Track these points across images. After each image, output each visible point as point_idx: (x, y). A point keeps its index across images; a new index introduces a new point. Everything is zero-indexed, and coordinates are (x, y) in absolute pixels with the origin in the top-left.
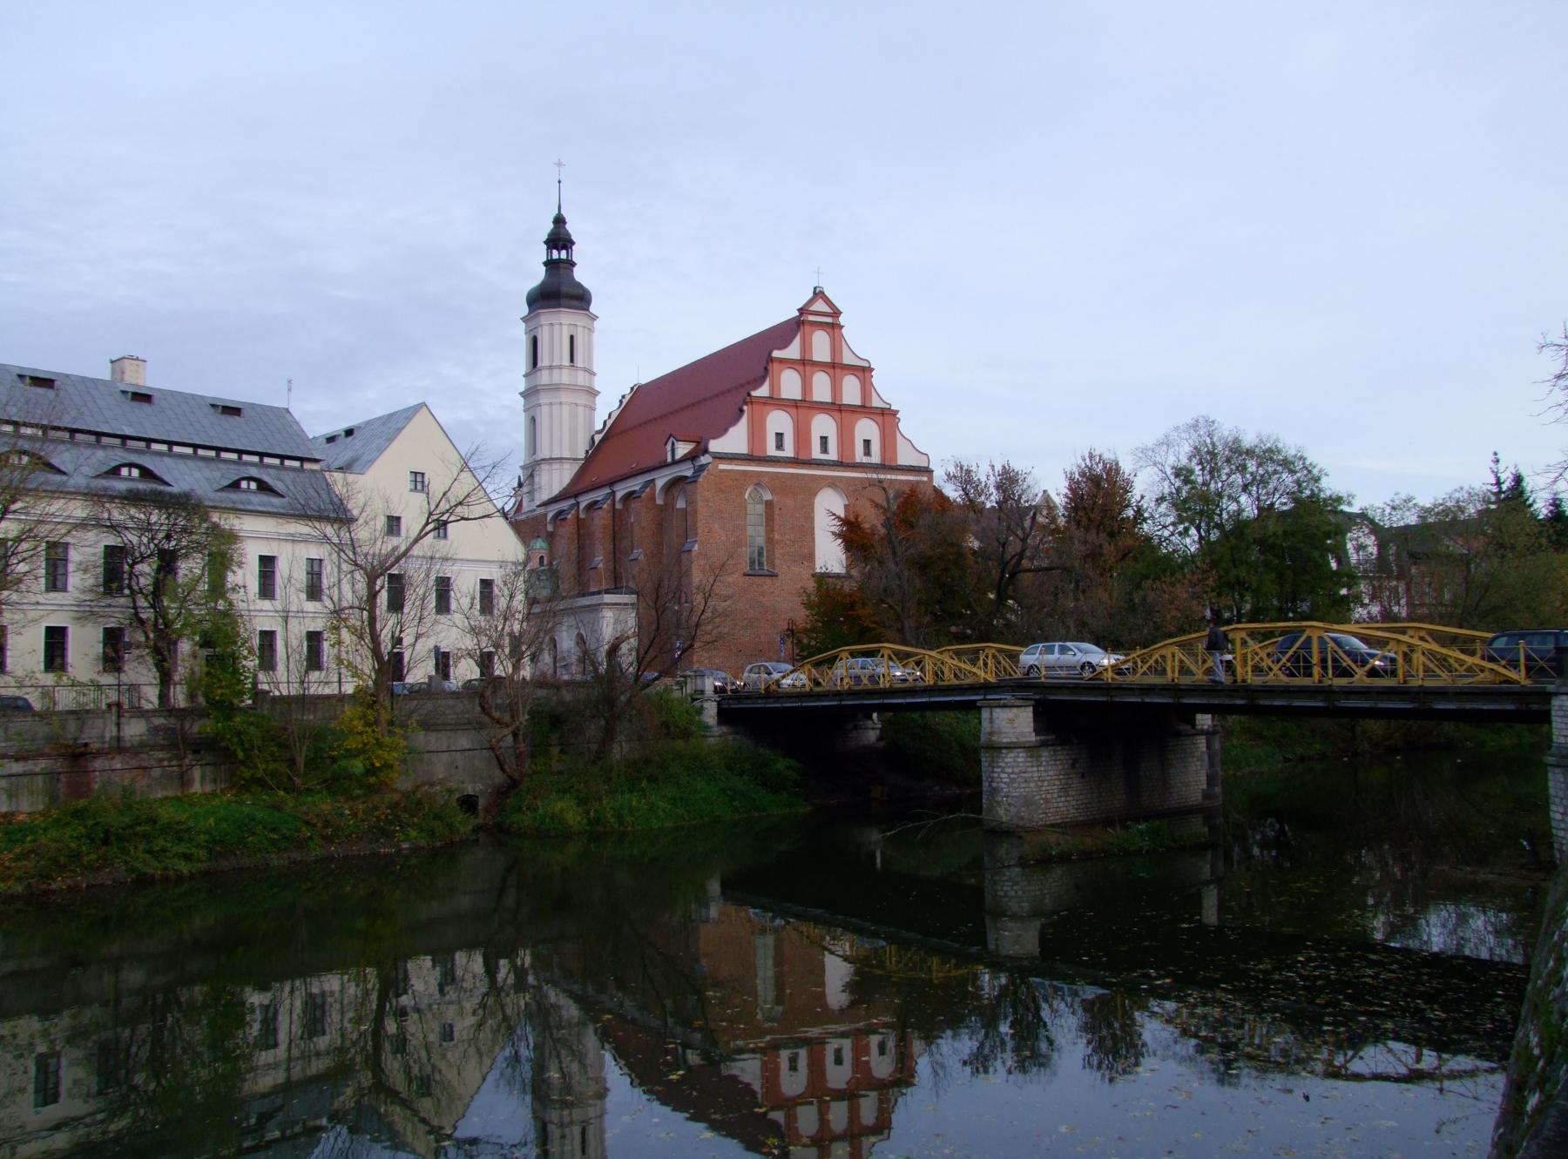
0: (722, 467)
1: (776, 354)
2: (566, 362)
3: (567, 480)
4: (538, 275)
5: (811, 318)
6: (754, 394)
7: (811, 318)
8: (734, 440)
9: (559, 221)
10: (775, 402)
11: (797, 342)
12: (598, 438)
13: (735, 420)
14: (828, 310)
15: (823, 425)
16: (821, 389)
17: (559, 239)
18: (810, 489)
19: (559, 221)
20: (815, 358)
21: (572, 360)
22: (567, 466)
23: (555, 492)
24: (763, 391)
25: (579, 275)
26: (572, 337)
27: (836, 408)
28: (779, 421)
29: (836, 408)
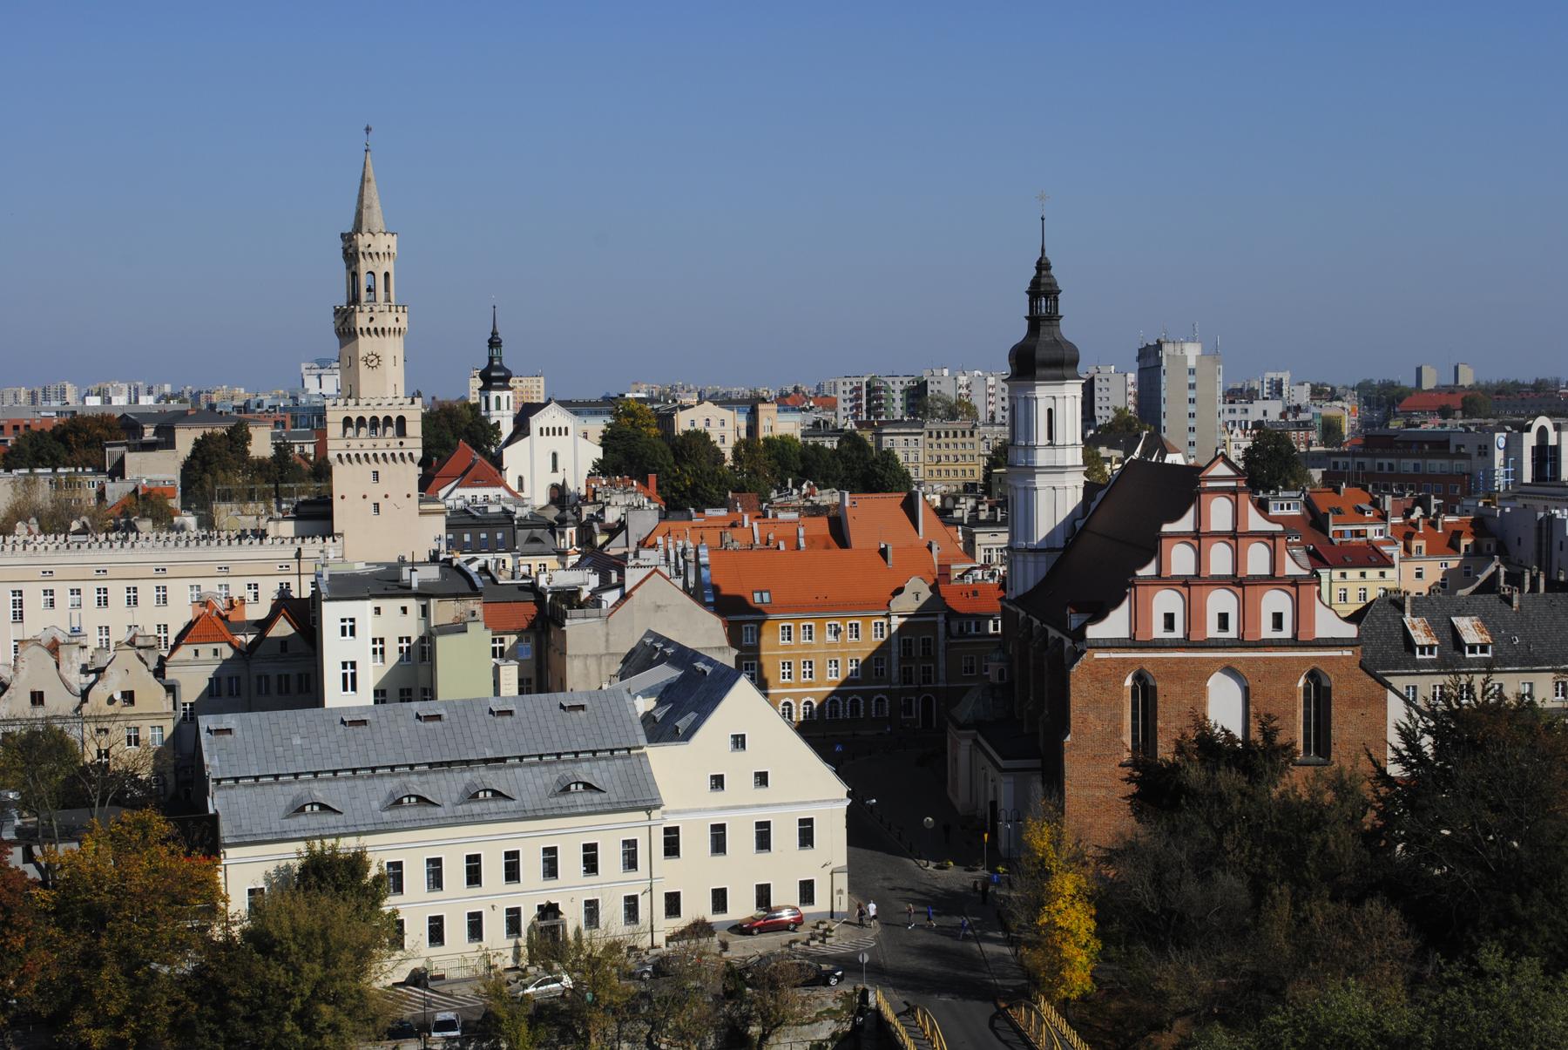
0: (1097, 656)
1: (1166, 528)
2: (1042, 439)
3: (1042, 573)
4: (1020, 331)
5: (1209, 484)
6: (1140, 573)
7: (1209, 484)
8: (1115, 624)
9: (1042, 266)
10: (1161, 580)
11: (1190, 515)
12: (1079, 524)
13: (1117, 604)
14: (1231, 473)
15: (1221, 601)
16: (1220, 560)
17: (1042, 289)
18: (1201, 674)
19: (1042, 266)
20: (1214, 527)
21: (1050, 436)
22: (1042, 558)
23: (1031, 586)
24: (1150, 570)
25: (1070, 327)
26: (1050, 411)
27: (1237, 581)
28: (1167, 601)
29: (1237, 581)
